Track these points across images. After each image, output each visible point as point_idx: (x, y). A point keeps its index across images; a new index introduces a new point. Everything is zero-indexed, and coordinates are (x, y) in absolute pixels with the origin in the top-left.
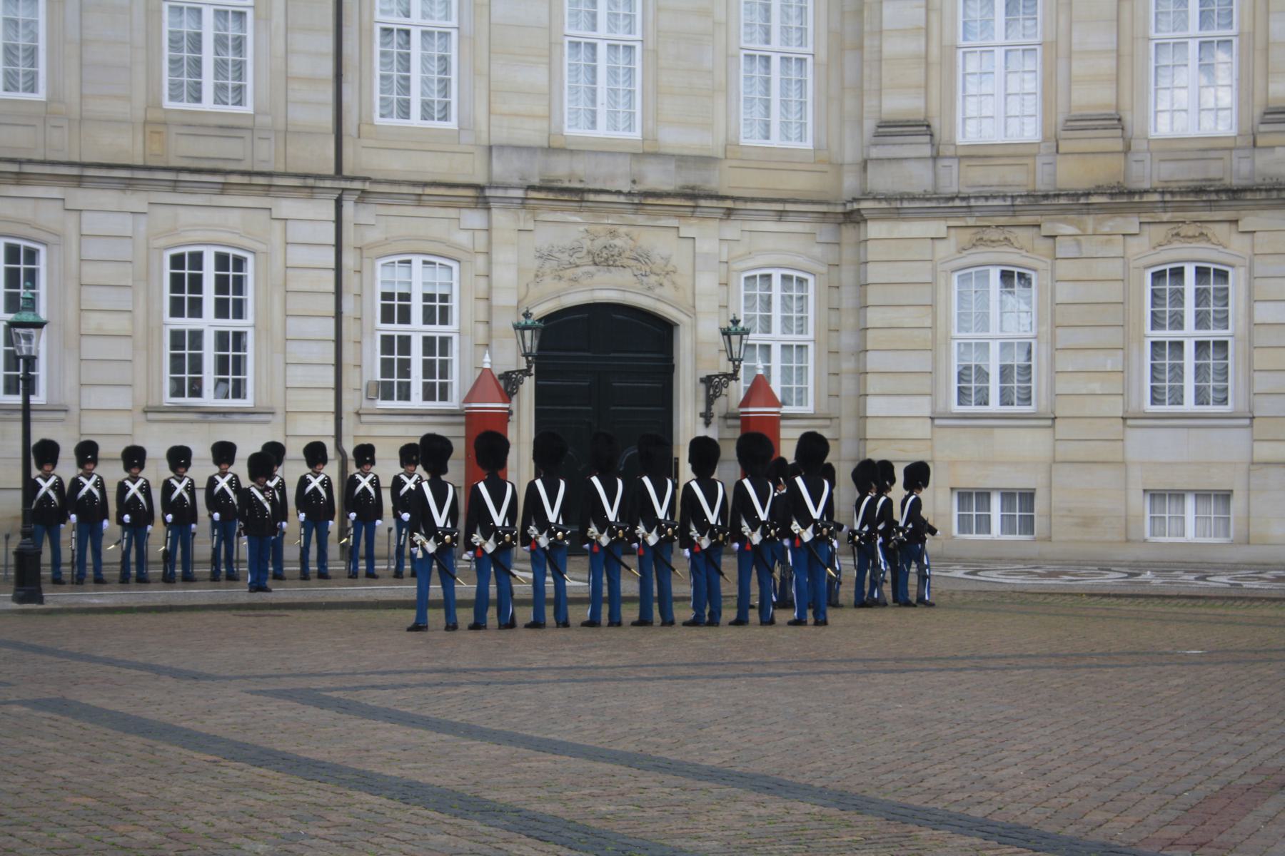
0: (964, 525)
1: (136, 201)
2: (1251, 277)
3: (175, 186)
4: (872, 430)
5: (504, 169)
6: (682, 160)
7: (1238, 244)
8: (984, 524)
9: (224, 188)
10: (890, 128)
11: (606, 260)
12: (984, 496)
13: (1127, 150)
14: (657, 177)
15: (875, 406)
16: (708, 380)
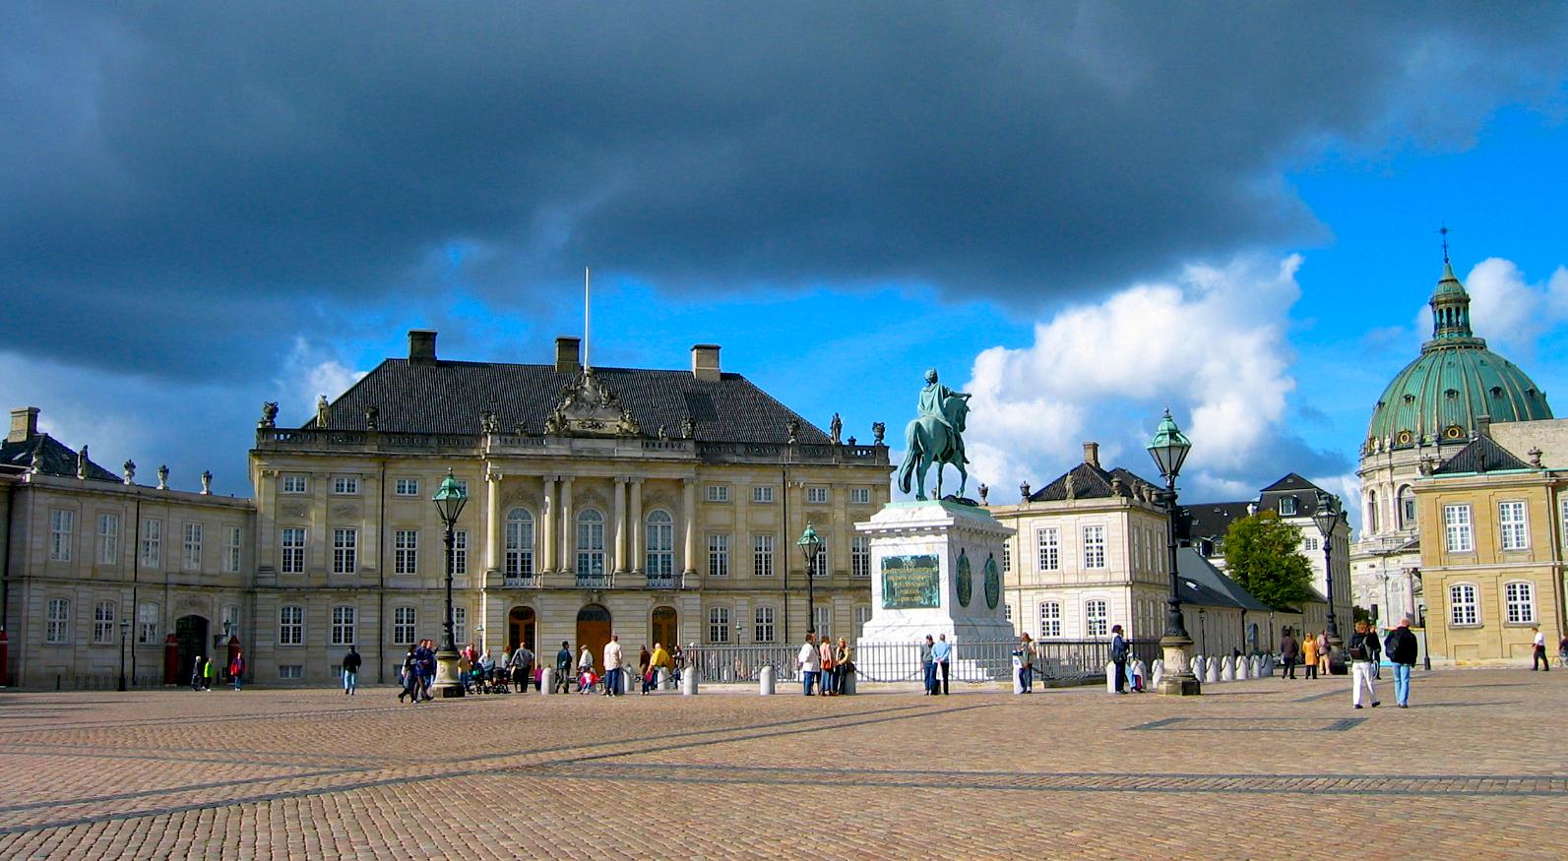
0: (282, 675)
1: (90, 589)
2: (359, 611)
3: (99, 585)
4: (257, 650)
5: (171, 579)
6: (214, 576)
7: (356, 602)
8: (287, 675)
9: (110, 585)
10: (263, 569)
11: (192, 604)
12: (288, 667)
13: (328, 576)
14: (206, 581)
15: (258, 644)
16: (215, 637)
